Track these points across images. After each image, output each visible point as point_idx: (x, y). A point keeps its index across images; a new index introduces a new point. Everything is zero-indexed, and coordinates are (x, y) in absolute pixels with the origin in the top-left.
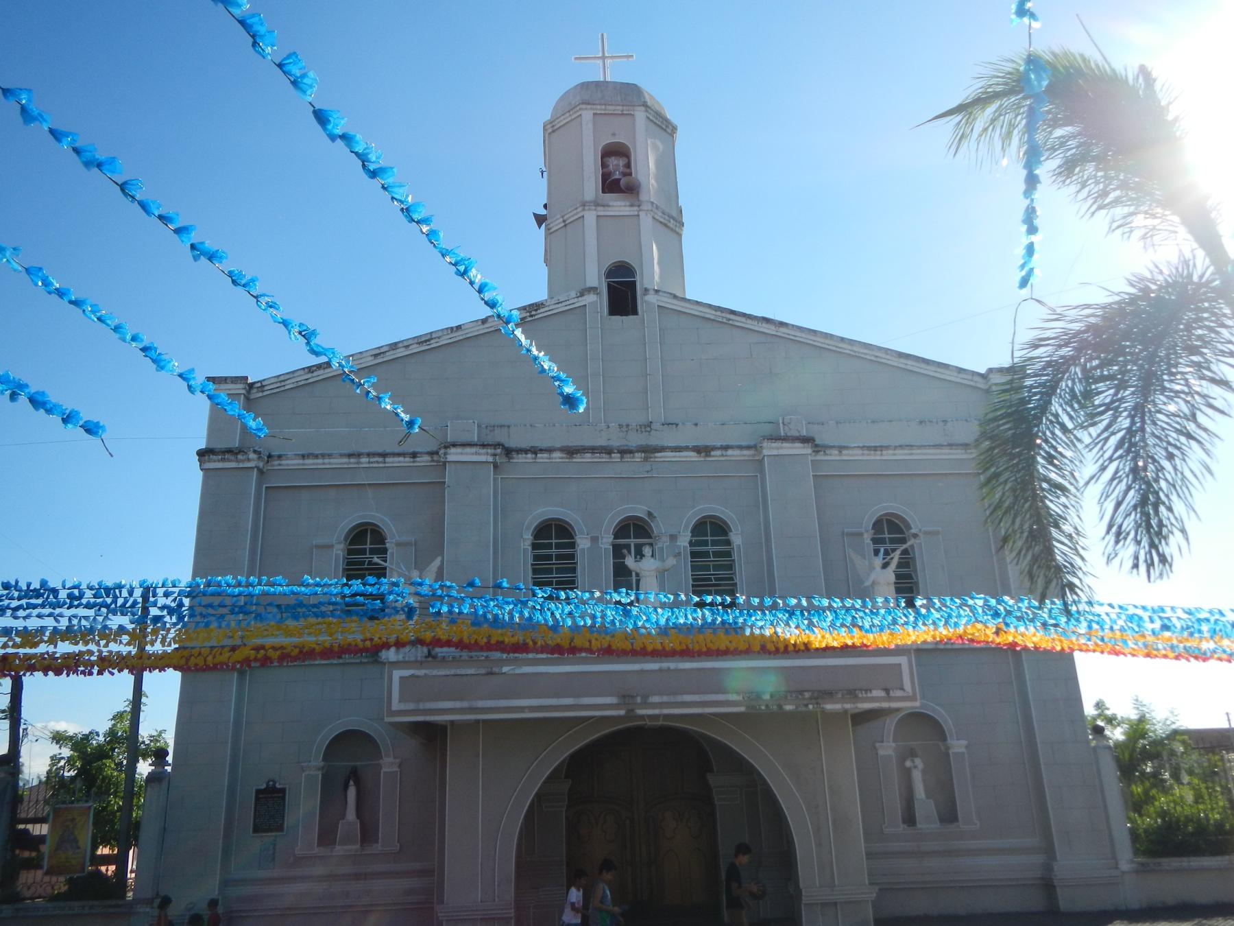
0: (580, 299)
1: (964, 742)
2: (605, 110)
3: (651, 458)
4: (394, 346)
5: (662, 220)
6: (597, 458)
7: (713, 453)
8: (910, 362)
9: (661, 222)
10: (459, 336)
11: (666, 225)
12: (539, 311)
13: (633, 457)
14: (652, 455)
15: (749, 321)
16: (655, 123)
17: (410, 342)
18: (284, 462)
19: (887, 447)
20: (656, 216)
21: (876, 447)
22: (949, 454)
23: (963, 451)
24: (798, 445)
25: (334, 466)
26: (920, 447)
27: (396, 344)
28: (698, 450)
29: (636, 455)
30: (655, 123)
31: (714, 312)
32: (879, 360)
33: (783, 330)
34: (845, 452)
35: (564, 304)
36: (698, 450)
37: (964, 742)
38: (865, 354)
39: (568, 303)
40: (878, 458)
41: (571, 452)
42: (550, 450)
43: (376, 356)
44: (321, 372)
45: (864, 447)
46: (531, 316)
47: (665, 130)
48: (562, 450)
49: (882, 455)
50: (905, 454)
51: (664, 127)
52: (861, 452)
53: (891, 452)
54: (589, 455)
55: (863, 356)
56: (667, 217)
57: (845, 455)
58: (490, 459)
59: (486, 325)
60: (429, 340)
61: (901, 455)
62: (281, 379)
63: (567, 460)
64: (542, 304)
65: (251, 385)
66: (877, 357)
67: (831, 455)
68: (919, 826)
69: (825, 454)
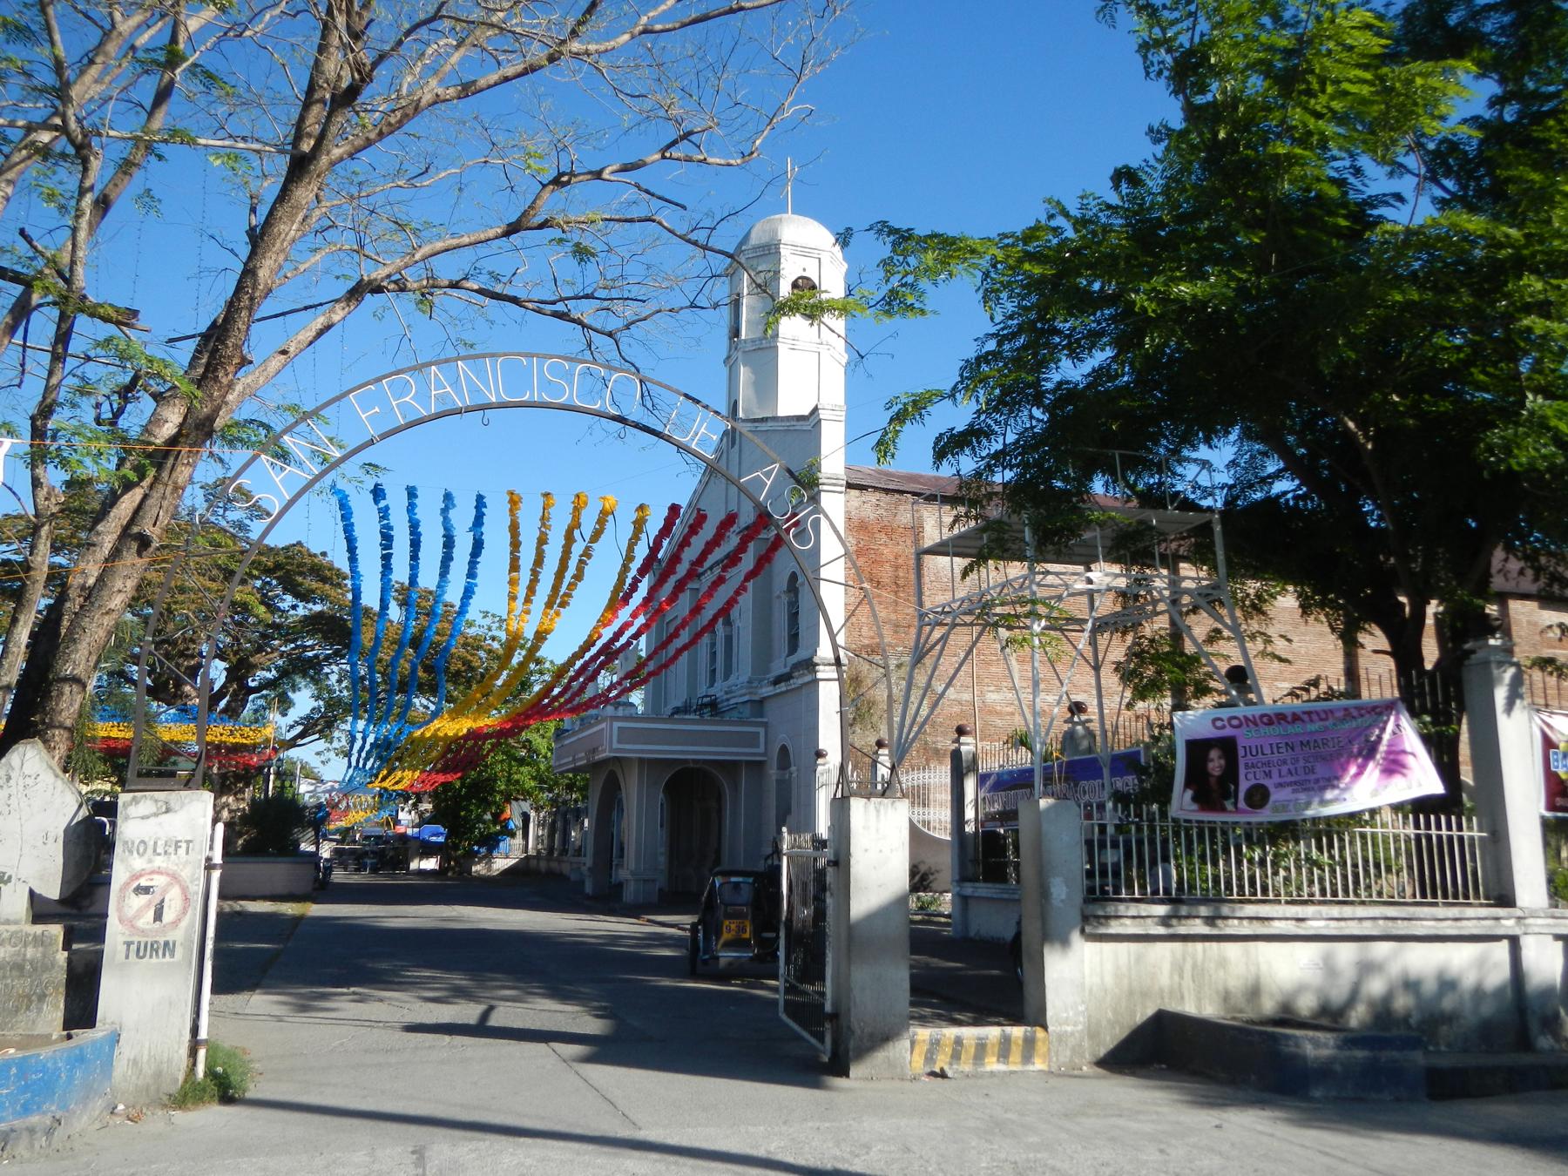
10: (697, 495)
33: (770, 424)
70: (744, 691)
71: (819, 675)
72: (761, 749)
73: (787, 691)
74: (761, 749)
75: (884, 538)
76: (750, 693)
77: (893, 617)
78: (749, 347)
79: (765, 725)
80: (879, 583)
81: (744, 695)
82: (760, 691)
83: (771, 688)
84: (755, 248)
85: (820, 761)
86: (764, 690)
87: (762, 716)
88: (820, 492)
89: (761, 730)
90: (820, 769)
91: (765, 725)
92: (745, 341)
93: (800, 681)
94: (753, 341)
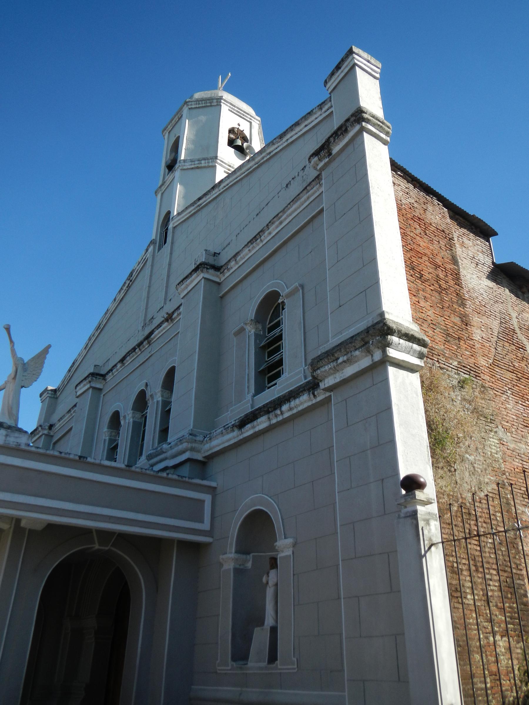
0: (147, 253)
1: (290, 541)
2: (172, 125)
3: (151, 341)
4: (90, 339)
5: (193, 166)
6: (134, 355)
7: (173, 317)
8: (288, 136)
9: (192, 168)
10: (108, 315)
11: (198, 168)
12: (133, 276)
13: (144, 347)
14: (150, 339)
15: (208, 197)
16: (199, 108)
17: (94, 331)
18: (57, 426)
19: (262, 231)
20: (185, 168)
21: (255, 237)
22: (308, 198)
23: (318, 185)
24: (195, 275)
25: (67, 420)
26: (283, 211)
27: (90, 337)
28: (167, 320)
29: (145, 343)
30: (199, 108)
31: (193, 208)
32: (272, 154)
33: (222, 185)
34: (238, 258)
35: (141, 263)
36: (167, 320)
37: (290, 541)
38: (263, 158)
39: (143, 260)
40: (261, 245)
41: (122, 361)
42: (115, 365)
43: (85, 348)
44: (73, 368)
45: (248, 243)
46: (131, 281)
47: (211, 106)
48: (119, 362)
49: (261, 241)
50: (277, 227)
51: (208, 104)
52: (248, 249)
53: (267, 233)
54: (128, 358)
55: (262, 161)
56: (197, 162)
57: (240, 261)
58: (88, 386)
59: (116, 301)
60: (99, 326)
61: (274, 230)
62: (63, 382)
63: (123, 367)
64: (133, 270)
65: (55, 391)
66: (270, 153)
67: (232, 268)
68: (250, 664)
69: (228, 270)
70: (185, 445)
71: (392, 353)
72: (206, 526)
73: (270, 428)
74: (206, 526)
75: (419, 231)
76: (192, 449)
77: (440, 319)
78: (188, 165)
79: (212, 490)
80: (422, 275)
81: (183, 452)
82: (207, 446)
83: (236, 432)
84: (198, 101)
85: (419, 495)
86: (214, 443)
87: (203, 478)
88: (363, 129)
89: (207, 498)
90: (420, 509)
91: (212, 490)
92: (184, 161)
93: (329, 382)
94: (192, 161)
